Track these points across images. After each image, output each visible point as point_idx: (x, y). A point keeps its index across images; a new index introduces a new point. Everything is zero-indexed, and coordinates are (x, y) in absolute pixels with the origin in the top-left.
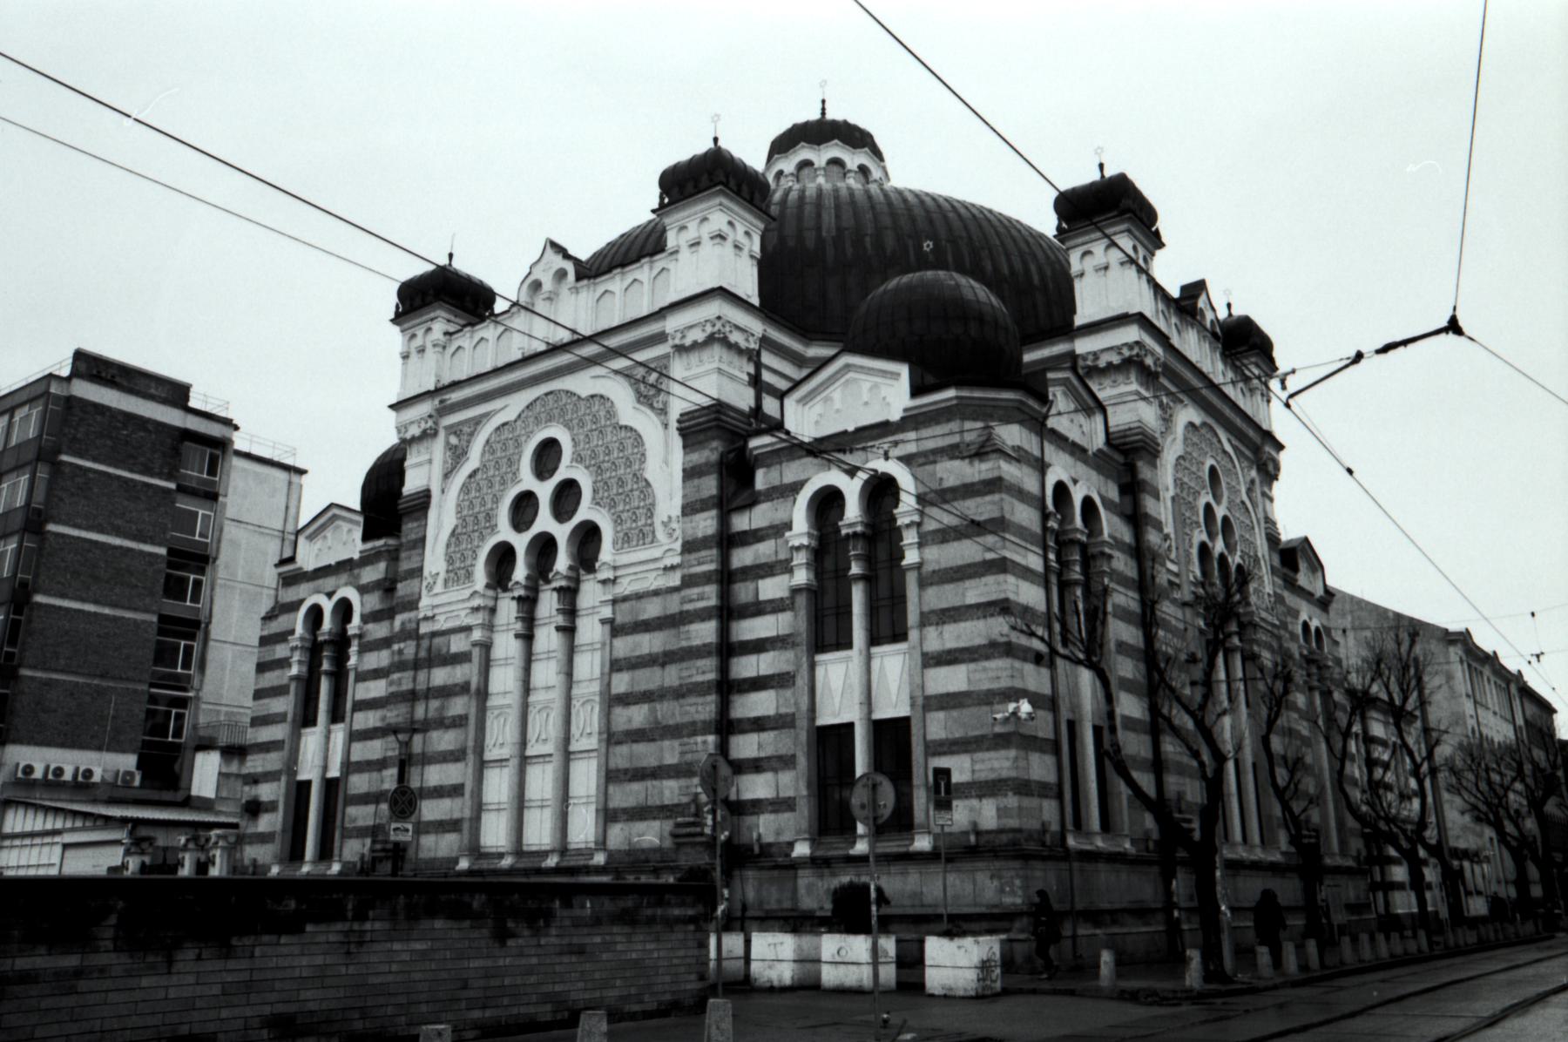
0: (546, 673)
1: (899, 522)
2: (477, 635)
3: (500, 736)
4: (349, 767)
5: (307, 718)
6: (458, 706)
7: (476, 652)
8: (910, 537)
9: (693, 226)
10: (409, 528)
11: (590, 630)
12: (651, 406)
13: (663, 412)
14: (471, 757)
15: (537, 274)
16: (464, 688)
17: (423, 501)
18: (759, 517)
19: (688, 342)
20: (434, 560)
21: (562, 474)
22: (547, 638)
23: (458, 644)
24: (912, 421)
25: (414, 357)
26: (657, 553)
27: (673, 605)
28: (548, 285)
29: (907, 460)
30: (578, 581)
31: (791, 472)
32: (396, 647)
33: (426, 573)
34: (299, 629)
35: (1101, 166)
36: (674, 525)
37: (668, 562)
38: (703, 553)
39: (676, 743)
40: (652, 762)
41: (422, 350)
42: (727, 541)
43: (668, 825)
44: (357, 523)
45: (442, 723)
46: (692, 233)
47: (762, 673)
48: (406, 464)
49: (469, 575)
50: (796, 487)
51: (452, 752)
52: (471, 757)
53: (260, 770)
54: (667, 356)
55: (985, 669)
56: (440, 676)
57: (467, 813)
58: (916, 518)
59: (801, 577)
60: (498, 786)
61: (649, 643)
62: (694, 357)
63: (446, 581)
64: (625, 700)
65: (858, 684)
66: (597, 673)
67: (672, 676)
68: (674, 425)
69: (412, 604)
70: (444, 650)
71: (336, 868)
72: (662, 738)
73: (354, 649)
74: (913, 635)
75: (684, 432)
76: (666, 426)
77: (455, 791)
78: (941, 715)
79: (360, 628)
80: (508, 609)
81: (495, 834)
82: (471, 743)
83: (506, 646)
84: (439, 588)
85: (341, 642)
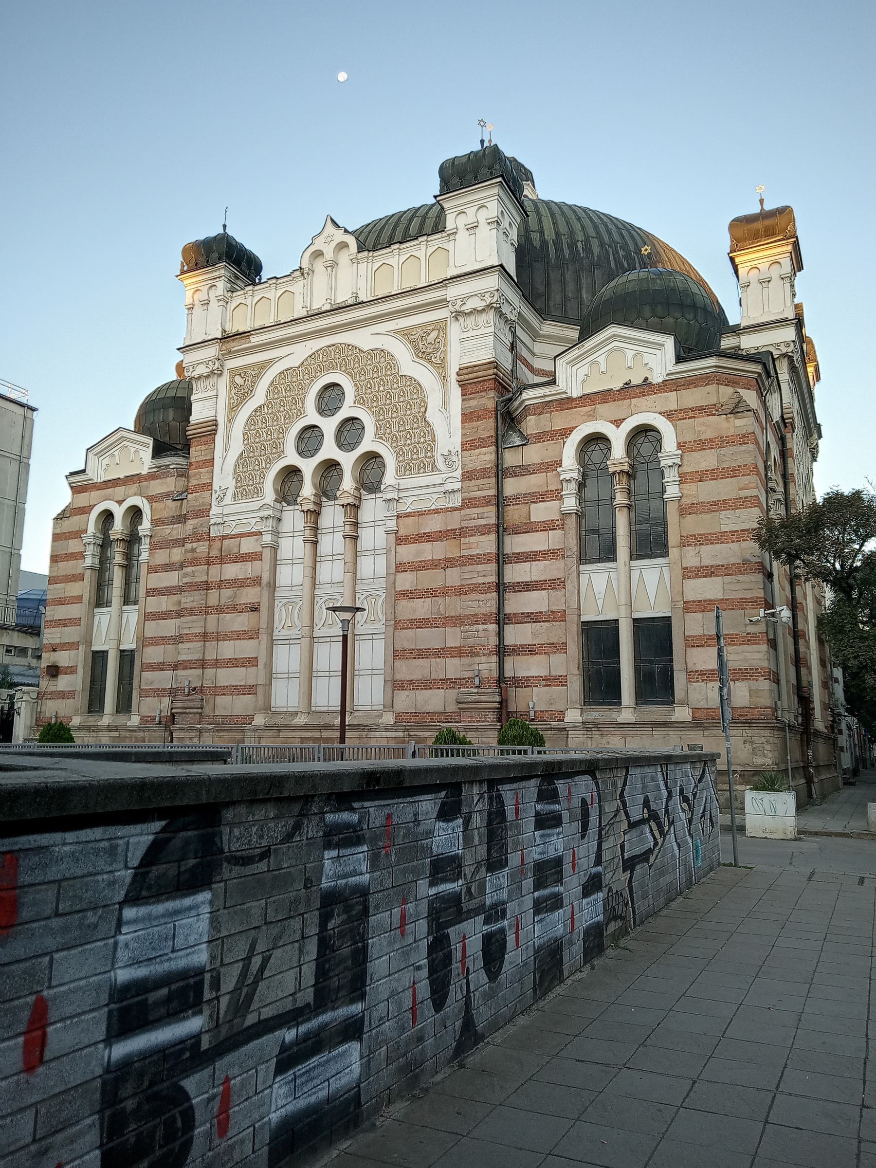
1: (663, 464)
2: (267, 538)
3: (287, 620)
4: (144, 641)
5: (100, 600)
6: (249, 595)
7: (267, 554)
8: (671, 476)
9: (471, 212)
10: (196, 452)
11: (373, 537)
12: (430, 361)
13: (441, 366)
14: (264, 637)
15: (319, 245)
16: (256, 581)
17: (210, 429)
18: (533, 454)
19: (467, 308)
20: (223, 477)
21: (344, 413)
22: (332, 543)
23: (248, 546)
24: (671, 385)
25: (198, 310)
26: (437, 479)
27: (454, 522)
28: (329, 254)
29: (669, 415)
30: (319, 505)
31: (559, 420)
32: (188, 546)
33: (215, 487)
34: (91, 529)
35: (761, 201)
36: (454, 458)
37: (449, 487)
39: (458, 629)
40: (437, 644)
41: (206, 303)
42: (500, 472)
43: (452, 694)
44: (145, 445)
45: (234, 608)
46: (470, 217)
47: (534, 578)
48: (193, 398)
49: (258, 491)
50: (566, 433)
51: (245, 632)
52: (264, 637)
53: (58, 641)
54: (445, 320)
55: (738, 582)
56: (232, 571)
57: (261, 680)
58: (678, 461)
59: (570, 503)
60: (287, 659)
61: (429, 551)
62: (470, 321)
63: (235, 496)
64: (407, 595)
65: (622, 590)
66: (383, 572)
67: (453, 577)
68: (454, 377)
69: (203, 512)
70: (236, 550)
71: (134, 720)
72: (444, 625)
73: (145, 545)
74: (673, 552)
75: (462, 384)
76: (445, 378)
77: (252, 662)
78: (699, 615)
79: (151, 530)
80: (294, 519)
81: (286, 696)
82: (263, 625)
83: (293, 546)
84: (228, 499)
85: (132, 540)
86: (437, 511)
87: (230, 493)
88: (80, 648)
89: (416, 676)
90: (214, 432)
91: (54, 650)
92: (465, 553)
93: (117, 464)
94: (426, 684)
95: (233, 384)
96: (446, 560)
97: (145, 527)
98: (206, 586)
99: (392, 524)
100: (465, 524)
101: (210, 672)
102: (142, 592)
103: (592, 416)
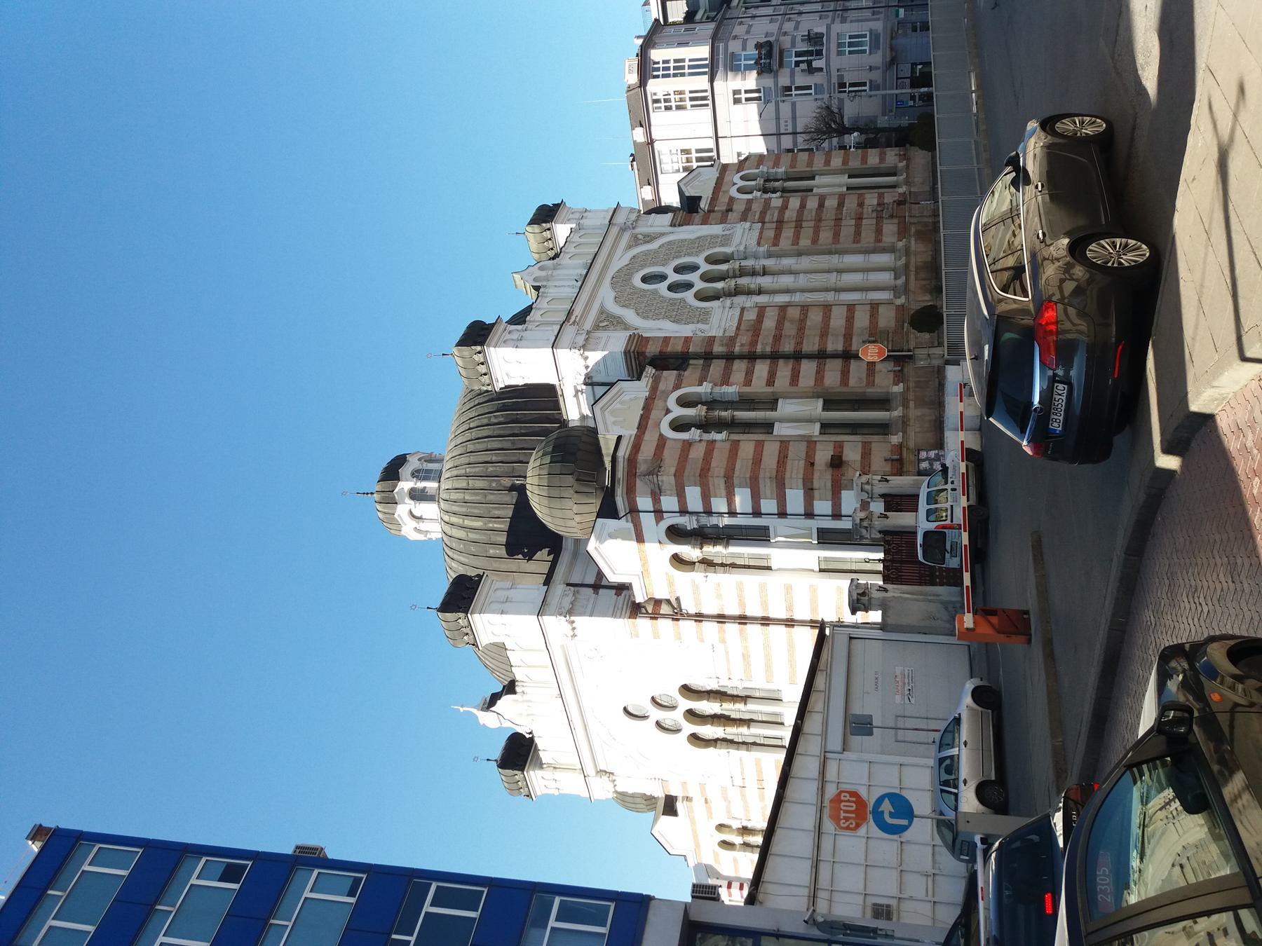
0: (786, 281)
13: (662, 235)
51: (825, 313)
53: (802, 463)
56: (769, 323)
61: (788, 233)
86: (761, 233)
87: (700, 326)
90: (640, 336)
91: (812, 464)
94: (879, 231)
95: (605, 328)
98: (777, 338)
99: (761, 249)
101: (855, 330)
102: (770, 389)
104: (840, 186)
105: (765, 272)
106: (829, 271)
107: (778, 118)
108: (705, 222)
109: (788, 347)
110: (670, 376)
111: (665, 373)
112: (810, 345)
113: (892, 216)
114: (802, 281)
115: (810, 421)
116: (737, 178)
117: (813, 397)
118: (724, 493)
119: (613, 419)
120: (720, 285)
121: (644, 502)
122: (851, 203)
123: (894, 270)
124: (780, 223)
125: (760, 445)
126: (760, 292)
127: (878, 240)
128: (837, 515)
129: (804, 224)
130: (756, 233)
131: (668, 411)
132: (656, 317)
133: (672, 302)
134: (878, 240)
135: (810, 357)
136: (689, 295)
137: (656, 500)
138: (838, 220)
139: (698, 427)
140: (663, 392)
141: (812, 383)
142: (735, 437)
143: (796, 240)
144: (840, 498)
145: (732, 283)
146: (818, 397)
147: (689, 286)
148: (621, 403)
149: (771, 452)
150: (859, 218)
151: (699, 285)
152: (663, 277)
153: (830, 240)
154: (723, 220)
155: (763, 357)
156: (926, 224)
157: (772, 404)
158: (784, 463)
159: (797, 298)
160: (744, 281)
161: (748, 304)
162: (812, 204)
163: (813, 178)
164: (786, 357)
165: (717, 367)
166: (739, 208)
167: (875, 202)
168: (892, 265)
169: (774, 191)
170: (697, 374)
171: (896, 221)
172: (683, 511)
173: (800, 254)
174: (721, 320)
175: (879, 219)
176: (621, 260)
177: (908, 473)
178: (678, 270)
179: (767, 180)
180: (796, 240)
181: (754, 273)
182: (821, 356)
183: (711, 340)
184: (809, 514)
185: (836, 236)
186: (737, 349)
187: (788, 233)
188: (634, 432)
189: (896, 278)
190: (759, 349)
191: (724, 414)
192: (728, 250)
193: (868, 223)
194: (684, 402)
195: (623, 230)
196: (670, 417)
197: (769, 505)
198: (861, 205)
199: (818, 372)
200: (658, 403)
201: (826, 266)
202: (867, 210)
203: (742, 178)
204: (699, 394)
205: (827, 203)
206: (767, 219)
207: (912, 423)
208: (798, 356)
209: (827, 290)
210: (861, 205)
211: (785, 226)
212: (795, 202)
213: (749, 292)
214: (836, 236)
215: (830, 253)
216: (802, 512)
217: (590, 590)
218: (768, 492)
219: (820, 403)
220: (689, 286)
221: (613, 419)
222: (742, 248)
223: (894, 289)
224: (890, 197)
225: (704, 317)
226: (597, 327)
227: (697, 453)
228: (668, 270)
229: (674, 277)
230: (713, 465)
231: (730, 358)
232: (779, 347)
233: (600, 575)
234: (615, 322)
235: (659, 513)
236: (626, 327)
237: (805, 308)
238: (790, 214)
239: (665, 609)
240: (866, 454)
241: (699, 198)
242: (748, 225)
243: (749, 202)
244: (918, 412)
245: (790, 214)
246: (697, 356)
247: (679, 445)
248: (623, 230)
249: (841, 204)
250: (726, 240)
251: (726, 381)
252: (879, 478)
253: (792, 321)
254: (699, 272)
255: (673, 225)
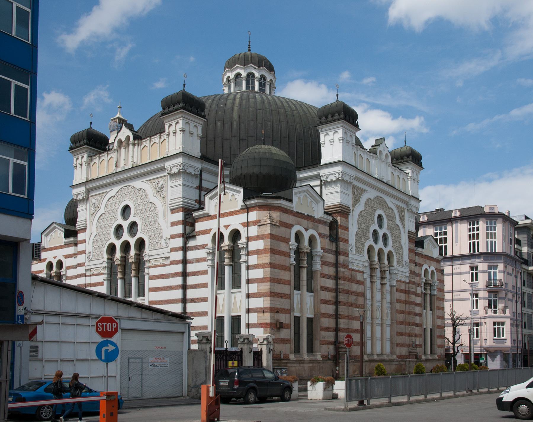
0: (378, 296)
13: (404, 226)
38: (413, 276)
53: (278, 306)
56: (355, 287)
61: (403, 297)
71: (319, 358)
78: (438, 329)
86: (403, 282)
88: (292, 313)
89: (400, 342)
91: (278, 312)
92: (410, 300)
93: (301, 204)
94: (402, 345)
96: (406, 301)
97: (318, 249)
98: (347, 292)
99: (395, 282)
100: (411, 290)
102: (319, 288)
103: (426, 263)
104: (426, 324)
105: (382, 284)
106: (382, 319)
107: (461, 291)
108: (410, 250)
109: (342, 298)
110: (326, 230)
111: (328, 228)
112: (343, 310)
113: (410, 352)
114: (377, 305)
115: (302, 311)
116: (432, 268)
117: (314, 312)
118: (261, 262)
119: (302, 197)
120: (376, 259)
121: (253, 215)
122: (417, 330)
123: (382, 354)
124: (408, 292)
125: (288, 283)
126: (372, 282)
127: (398, 345)
128: (248, 326)
129: (407, 306)
130: (403, 279)
131: (306, 230)
132: (360, 222)
133: (367, 231)
134: (398, 345)
135: (337, 310)
136: (371, 242)
137: (255, 223)
138: (409, 324)
139: (298, 247)
140: (318, 226)
141: (323, 311)
142: (292, 269)
143: (399, 301)
144: (258, 327)
145: (377, 267)
146: (315, 315)
147: (376, 241)
148: (311, 202)
149: (285, 289)
150: (409, 335)
151: (377, 248)
152: (381, 226)
153: (398, 320)
154: (411, 261)
155: (337, 284)
156: (405, 370)
157: (310, 289)
158: (278, 297)
159: (369, 302)
160: (378, 273)
161: (365, 276)
162: (418, 310)
163: (431, 310)
164: (337, 297)
165: (331, 258)
166: (417, 270)
167: (417, 343)
168: (384, 353)
169: (425, 289)
170: (327, 247)
171: (407, 354)
172: (248, 239)
173: (391, 303)
174: (357, 260)
175: (409, 345)
176: (389, 201)
177: (273, 363)
178: (385, 235)
179: (431, 286)
180: (399, 301)
181: (382, 278)
182: (337, 316)
183: (346, 255)
184: (248, 311)
185: (401, 323)
186: (341, 269)
187: (403, 297)
188: (295, 210)
189: (377, 355)
190: (341, 282)
191: (305, 262)
192: (395, 263)
193: (406, 340)
194: (312, 240)
195: (407, 203)
196: (303, 231)
197: (253, 288)
198: (416, 336)
199: (328, 314)
200: (311, 224)
201: (385, 318)
202: (414, 339)
203: (432, 271)
204: (316, 248)
205: (418, 318)
206: (411, 285)
207: (301, 365)
208: (337, 303)
209: (372, 318)
210: (416, 336)
211: (407, 295)
212: (419, 300)
213: (372, 276)
214: (401, 323)
215: (392, 320)
216: (249, 307)
217: (198, 184)
218: (261, 288)
219: (311, 316)
220: (376, 241)
221: (302, 197)
222: (396, 272)
223: (372, 354)
224: (419, 350)
225: (359, 250)
226: (354, 187)
227: (283, 247)
228: (384, 230)
229: (381, 233)
230: (277, 256)
231: (336, 265)
232: (342, 291)
233: (209, 191)
234: (356, 200)
235: (247, 225)
236: (354, 206)
237: (363, 306)
238: (413, 298)
239: (188, 229)
240: (284, 341)
241: (423, 247)
242: (408, 275)
243: (420, 275)
244: (306, 368)
245: (413, 298)
246: (337, 246)
247: (287, 237)
248: (407, 203)
249: (417, 325)
250: (400, 262)
251: (324, 263)
252: (272, 348)
253: (356, 300)
254: (383, 247)
255: (409, 232)
